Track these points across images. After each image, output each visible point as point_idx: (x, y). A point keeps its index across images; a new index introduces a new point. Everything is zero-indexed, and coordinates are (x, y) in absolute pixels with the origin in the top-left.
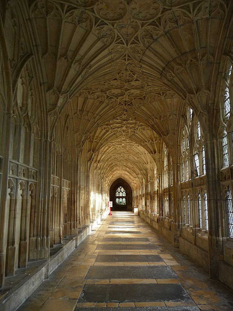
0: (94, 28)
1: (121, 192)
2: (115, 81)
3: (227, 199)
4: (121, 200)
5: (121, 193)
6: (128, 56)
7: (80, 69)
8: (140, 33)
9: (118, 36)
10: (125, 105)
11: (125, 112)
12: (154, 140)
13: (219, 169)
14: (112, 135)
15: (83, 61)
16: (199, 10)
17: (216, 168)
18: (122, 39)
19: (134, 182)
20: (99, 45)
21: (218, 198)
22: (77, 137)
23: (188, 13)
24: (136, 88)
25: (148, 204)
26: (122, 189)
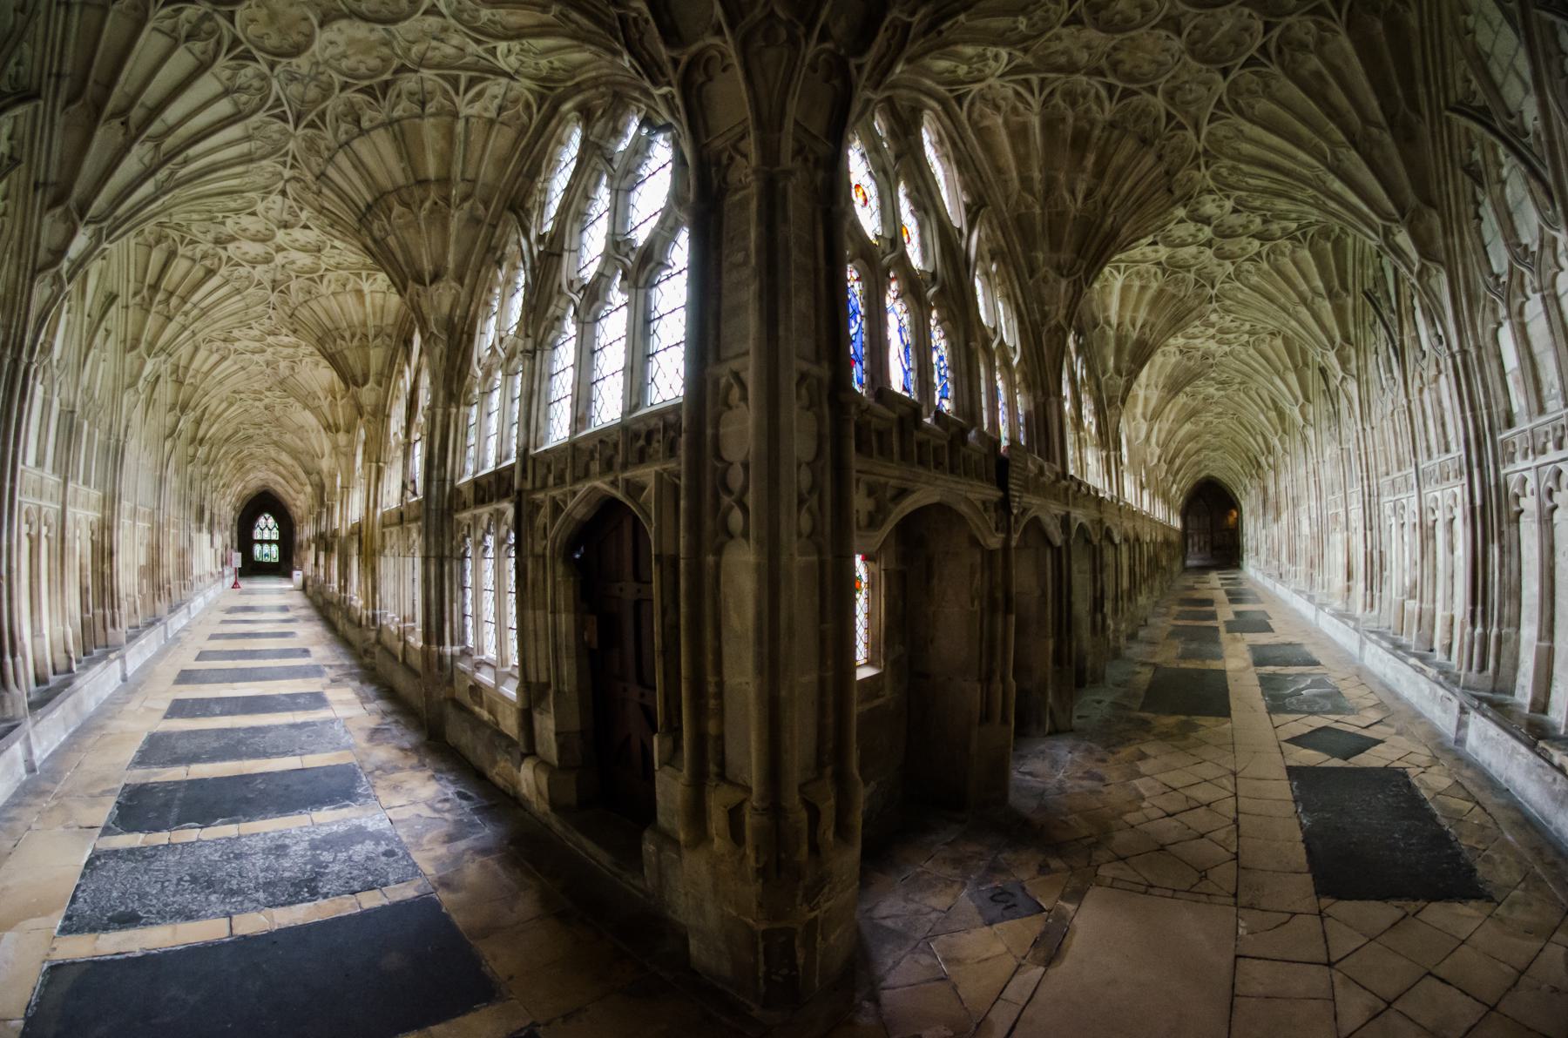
0: (222, 61)
1: (267, 528)
2: (254, 218)
3: (464, 557)
4: (266, 547)
5: (266, 531)
6: (294, 157)
7: (156, 161)
8: (334, 104)
9: (278, 99)
10: (273, 291)
11: (270, 311)
12: (338, 397)
13: (453, 481)
14: (235, 372)
15: (170, 142)
16: (480, 95)
17: (448, 477)
18: (286, 108)
19: (300, 500)
20: (224, 108)
21: (447, 553)
22: (132, 363)
23: (452, 93)
24: (303, 249)
25: (322, 561)
26: (271, 522)
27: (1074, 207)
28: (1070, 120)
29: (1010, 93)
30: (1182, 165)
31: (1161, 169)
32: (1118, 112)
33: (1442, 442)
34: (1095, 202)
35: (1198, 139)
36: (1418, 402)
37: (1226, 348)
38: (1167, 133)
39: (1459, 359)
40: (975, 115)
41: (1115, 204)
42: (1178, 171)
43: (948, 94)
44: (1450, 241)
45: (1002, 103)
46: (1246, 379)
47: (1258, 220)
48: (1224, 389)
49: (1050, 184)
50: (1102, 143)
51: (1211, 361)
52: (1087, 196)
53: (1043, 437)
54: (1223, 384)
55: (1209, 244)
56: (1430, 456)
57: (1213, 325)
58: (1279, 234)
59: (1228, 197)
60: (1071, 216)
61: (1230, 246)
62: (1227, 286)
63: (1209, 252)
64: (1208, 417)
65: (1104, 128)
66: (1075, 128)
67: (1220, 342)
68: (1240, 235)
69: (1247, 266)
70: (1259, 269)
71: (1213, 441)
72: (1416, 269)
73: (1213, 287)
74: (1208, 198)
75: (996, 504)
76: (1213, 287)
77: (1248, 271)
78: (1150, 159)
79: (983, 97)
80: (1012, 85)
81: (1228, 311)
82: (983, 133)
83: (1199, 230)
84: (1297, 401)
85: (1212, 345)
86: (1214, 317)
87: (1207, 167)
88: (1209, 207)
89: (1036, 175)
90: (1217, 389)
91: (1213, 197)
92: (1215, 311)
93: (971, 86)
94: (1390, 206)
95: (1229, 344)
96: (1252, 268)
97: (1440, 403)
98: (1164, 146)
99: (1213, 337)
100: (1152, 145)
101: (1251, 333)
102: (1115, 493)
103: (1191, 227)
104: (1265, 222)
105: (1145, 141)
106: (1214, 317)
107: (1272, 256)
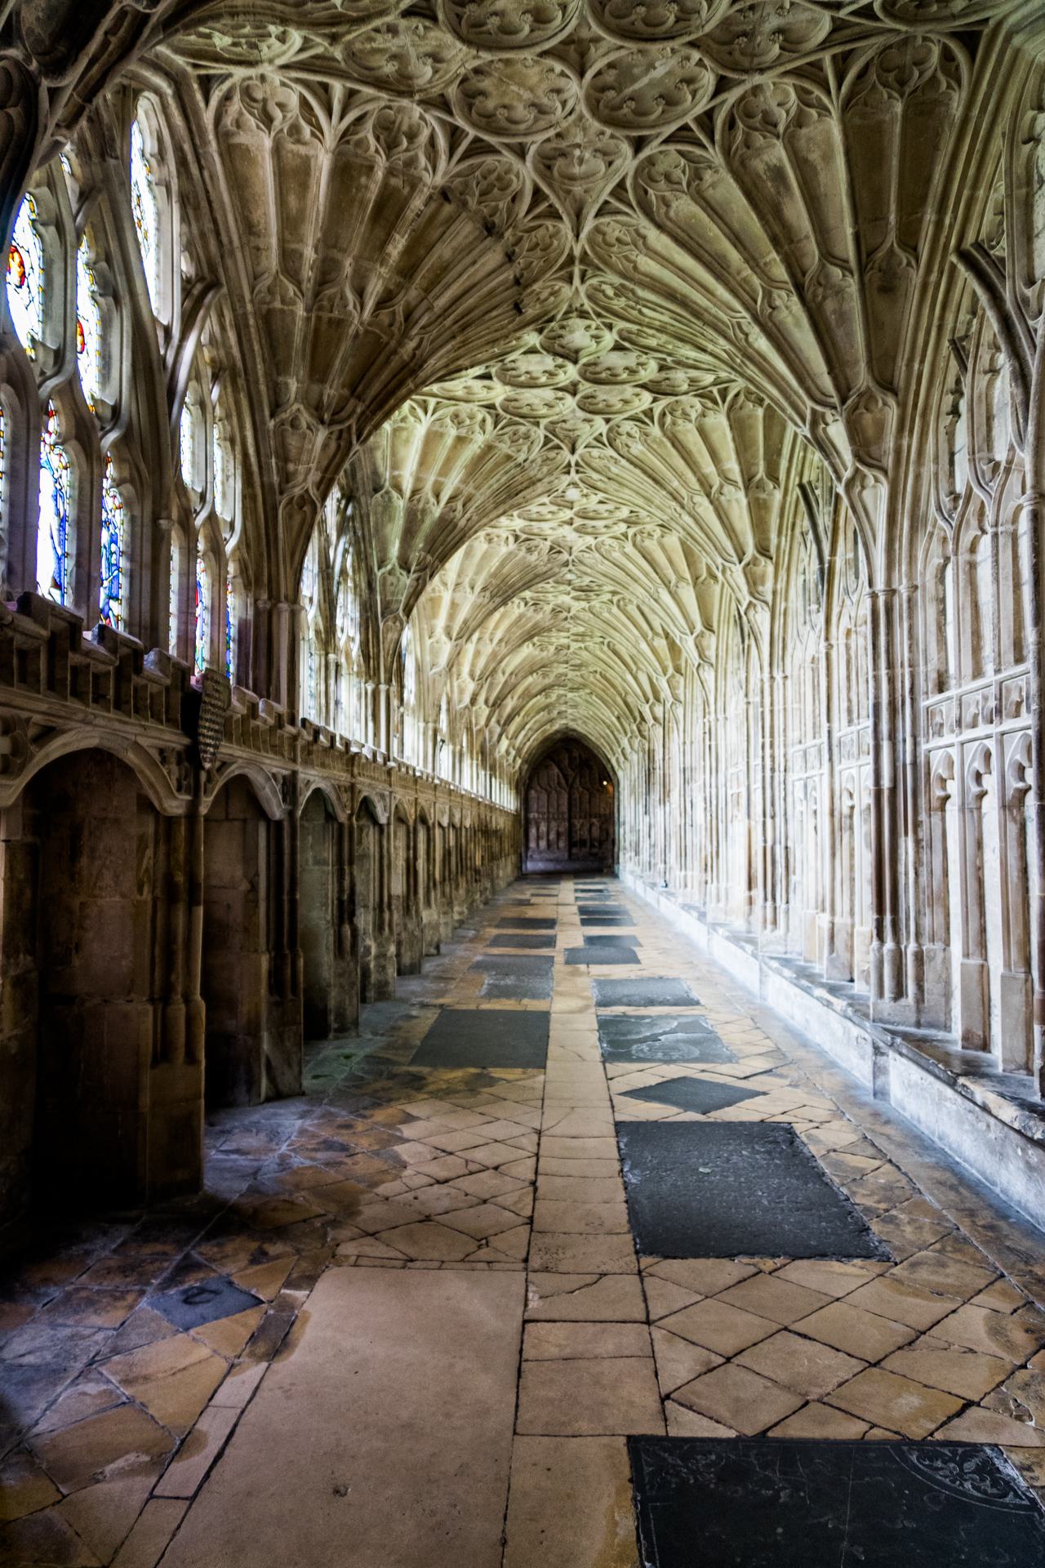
27: (360, 317)
28: (379, 174)
29: (294, 102)
30: (543, 272)
31: (509, 274)
32: (458, 175)
34: (394, 313)
35: (577, 236)
36: (842, 649)
37: (590, 540)
38: (527, 222)
40: (228, 121)
41: (423, 322)
42: (535, 280)
43: (189, 69)
44: (905, 443)
45: (278, 114)
46: (619, 588)
47: (653, 365)
48: (588, 600)
49: (327, 272)
50: (422, 220)
51: (565, 556)
52: (381, 304)
53: (263, 662)
55: (573, 390)
57: (570, 505)
58: (685, 387)
59: (610, 327)
60: (351, 331)
61: (606, 395)
62: (595, 452)
63: (570, 402)
65: (430, 197)
66: (385, 185)
67: (581, 531)
68: (623, 383)
69: (628, 426)
70: (647, 435)
71: (571, 674)
72: (847, 475)
73: (573, 451)
74: (577, 323)
75: (179, 754)
76: (573, 451)
77: (629, 435)
78: (494, 258)
79: (247, 93)
80: (299, 88)
82: (233, 154)
83: (561, 367)
85: (568, 533)
86: (573, 494)
87: (583, 281)
88: (579, 335)
89: (309, 254)
90: (577, 599)
91: (588, 322)
92: (575, 485)
93: (232, 69)
94: (827, 383)
95: (596, 535)
96: (635, 432)
98: (519, 240)
100: (501, 236)
101: (629, 522)
102: (383, 749)
103: (549, 362)
104: (662, 368)
105: (490, 229)
107: (669, 419)
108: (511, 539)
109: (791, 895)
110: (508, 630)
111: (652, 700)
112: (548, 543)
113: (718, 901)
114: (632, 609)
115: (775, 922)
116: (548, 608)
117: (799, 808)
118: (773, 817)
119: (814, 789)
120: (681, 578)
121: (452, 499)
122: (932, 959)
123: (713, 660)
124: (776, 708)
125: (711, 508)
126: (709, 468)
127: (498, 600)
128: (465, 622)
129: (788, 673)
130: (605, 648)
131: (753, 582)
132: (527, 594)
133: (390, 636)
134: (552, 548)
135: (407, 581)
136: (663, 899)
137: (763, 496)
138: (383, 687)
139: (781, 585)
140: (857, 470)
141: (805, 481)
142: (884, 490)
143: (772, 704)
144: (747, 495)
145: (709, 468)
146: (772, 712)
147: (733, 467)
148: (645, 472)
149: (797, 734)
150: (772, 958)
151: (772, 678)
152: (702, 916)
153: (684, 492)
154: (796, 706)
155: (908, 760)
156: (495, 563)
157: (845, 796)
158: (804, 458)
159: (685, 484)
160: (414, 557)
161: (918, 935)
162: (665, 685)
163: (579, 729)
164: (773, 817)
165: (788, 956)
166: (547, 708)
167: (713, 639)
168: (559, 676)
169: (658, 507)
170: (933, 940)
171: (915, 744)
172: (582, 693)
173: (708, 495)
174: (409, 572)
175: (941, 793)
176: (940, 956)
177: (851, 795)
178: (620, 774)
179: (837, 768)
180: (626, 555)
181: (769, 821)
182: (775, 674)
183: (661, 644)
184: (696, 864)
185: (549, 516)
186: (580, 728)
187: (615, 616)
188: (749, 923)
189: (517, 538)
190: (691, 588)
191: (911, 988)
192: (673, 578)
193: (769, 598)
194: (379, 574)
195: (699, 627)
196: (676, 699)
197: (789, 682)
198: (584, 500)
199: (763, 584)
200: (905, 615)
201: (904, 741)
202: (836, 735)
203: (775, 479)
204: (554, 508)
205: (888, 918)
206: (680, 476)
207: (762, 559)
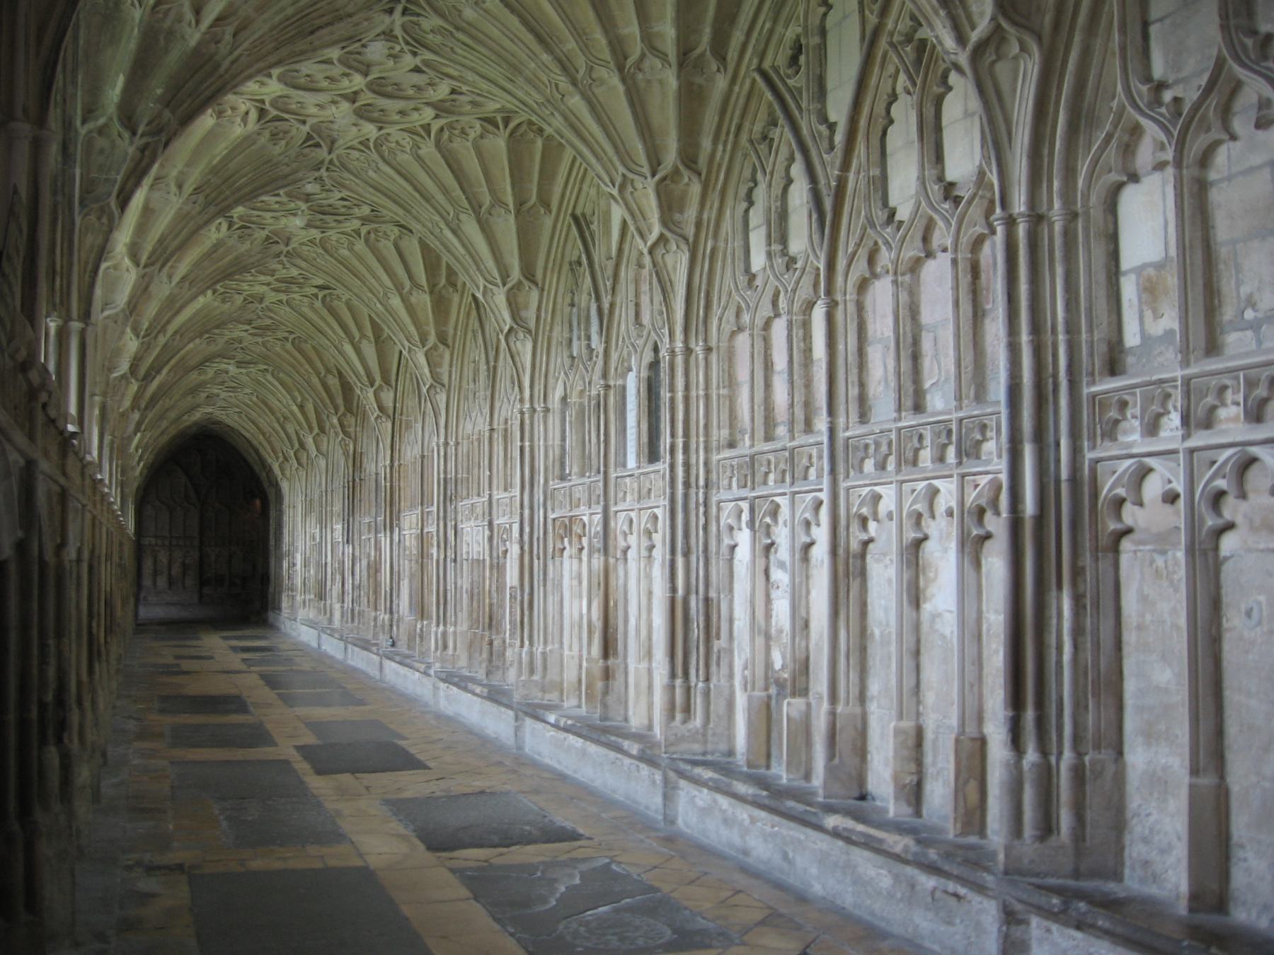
33: (909, 387)
36: (851, 308)
37: (370, 130)
39: (1022, 230)
51: (323, 153)
54: (322, 214)
56: (864, 417)
64: (256, 285)
67: (363, 113)
71: (248, 340)
81: (417, 43)
84: (505, 277)
92: (388, 35)
95: (381, 123)
97: (914, 311)
99: (353, 98)
101: (441, 108)
106: (376, 50)
108: (253, 115)
109: (714, 668)
110: (197, 265)
111: (378, 381)
112: (306, 129)
113: (532, 671)
114: (387, 247)
115: (687, 709)
116: (261, 235)
117: (727, 541)
118: (686, 554)
119: (775, 512)
120: (498, 201)
121: (220, 20)
122: (1098, 775)
123: (532, 325)
124: (693, 393)
125: (621, 88)
126: (631, 29)
127: (212, 209)
128: (161, 241)
129: (713, 343)
130: (318, 304)
131: (670, 206)
132: (239, 210)
133: (89, 239)
134: (309, 137)
135: (128, 147)
136: (390, 666)
137: (699, 80)
138: (76, 325)
139: (710, 214)
140: (998, 28)
141: (767, 65)
142: (1031, 67)
143: (687, 387)
144: (679, 77)
145: (631, 29)
146: (687, 399)
147: (668, 31)
148: (524, 22)
149: (725, 432)
150: (695, 763)
151: (688, 351)
152: (496, 696)
153: (581, 62)
154: (722, 392)
155: (1064, 474)
156: (221, 149)
157: (855, 527)
158: (771, 31)
159: (585, 45)
160: (148, 108)
161: (1077, 739)
162: (422, 360)
163: (229, 421)
164: (686, 554)
165: (709, 757)
166: (194, 391)
167: (535, 294)
168: (230, 342)
169: (529, 81)
170: (1097, 747)
171: (1076, 451)
172: (253, 369)
173: (621, 68)
174: (134, 133)
175: (1113, 526)
176: (1111, 769)
177: (864, 521)
178: (285, 486)
179: (843, 485)
180: (419, 159)
181: (680, 561)
182: (692, 345)
183: (423, 300)
184: (463, 615)
185: (325, 84)
186: (231, 418)
187: (360, 259)
188: (605, 706)
189: (262, 112)
190: (512, 218)
191: (1065, 819)
192: (487, 200)
193: (690, 231)
194: (83, 131)
195: (516, 274)
196: (435, 376)
197: (714, 357)
198: (391, 63)
199: (681, 212)
200: (1058, 254)
201: (1058, 444)
202: (842, 435)
203: (722, 58)
204: (337, 70)
205: (1030, 715)
206: (580, 35)
207: (686, 174)
